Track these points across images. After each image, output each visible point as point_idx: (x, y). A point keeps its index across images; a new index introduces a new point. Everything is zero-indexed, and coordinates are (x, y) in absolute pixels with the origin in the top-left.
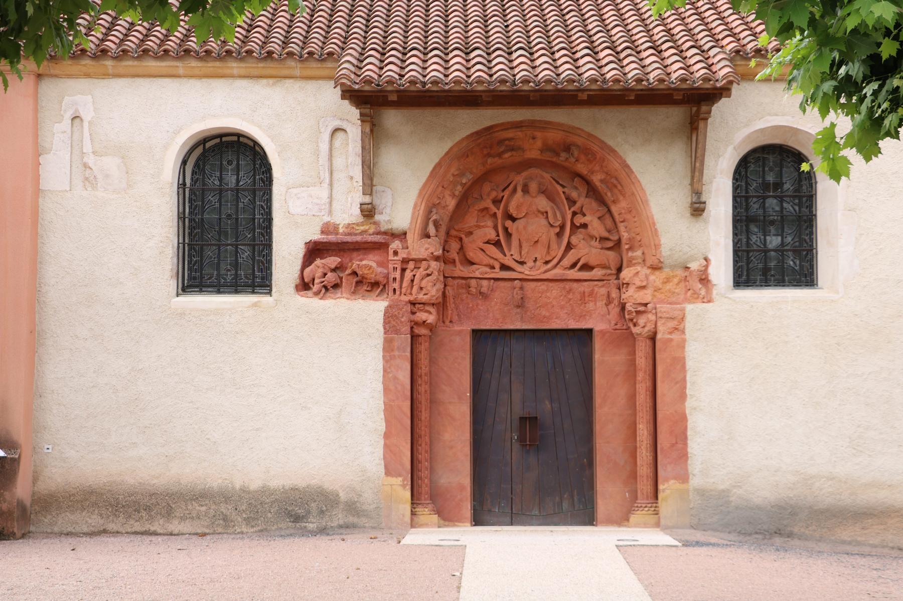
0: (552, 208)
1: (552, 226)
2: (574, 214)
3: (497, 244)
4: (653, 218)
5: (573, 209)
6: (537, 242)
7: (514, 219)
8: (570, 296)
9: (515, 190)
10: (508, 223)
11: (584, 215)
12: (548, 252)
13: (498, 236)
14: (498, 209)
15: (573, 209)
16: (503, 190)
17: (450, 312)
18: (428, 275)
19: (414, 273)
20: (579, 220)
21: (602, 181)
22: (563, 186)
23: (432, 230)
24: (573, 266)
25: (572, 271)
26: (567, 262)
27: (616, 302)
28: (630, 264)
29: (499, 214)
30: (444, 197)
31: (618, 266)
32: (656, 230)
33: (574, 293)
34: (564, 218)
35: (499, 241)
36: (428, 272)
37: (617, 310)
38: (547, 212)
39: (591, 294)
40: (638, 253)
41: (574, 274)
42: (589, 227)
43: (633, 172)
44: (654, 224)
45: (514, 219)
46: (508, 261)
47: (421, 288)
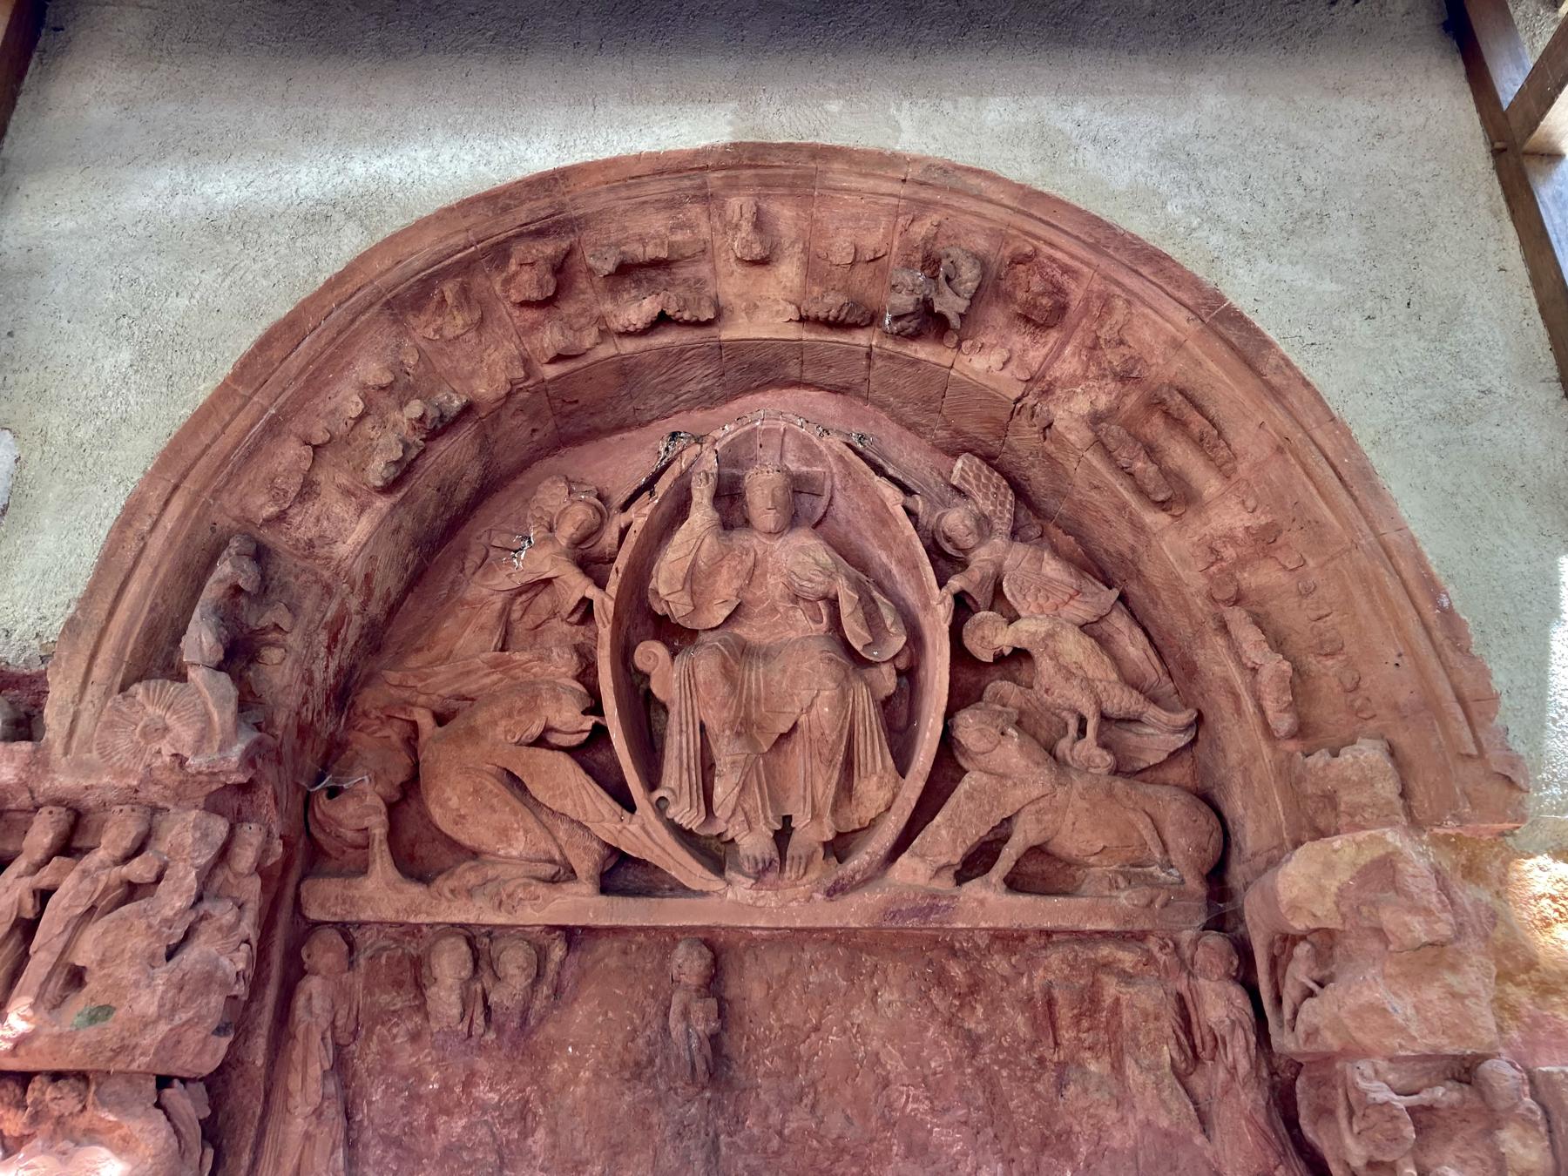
0: (858, 586)
1: (857, 660)
2: (963, 606)
3: (590, 751)
4: (1418, 557)
5: (956, 583)
6: (785, 737)
7: (676, 635)
8: (975, 1021)
9: (679, 509)
10: (651, 655)
11: (1013, 617)
12: (846, 787)
13: (596, 708)
14: (601, 584)
15: (956, 583)
16: (625, 507)
17: (299, 1124)
18: (132, 891)
19: (45, 878)
20: (991, 636)
21: (1096, 419)
22: (907, 491)
23: (201, 639)
24: (977, 861)
25: (974, 888)
26: (947, 836)
27: (1239, 1051)
28: (1314, 819)
29: (605, 602)
30: (308, 489)
31: (1212, 854)
32: (1448, 615)
33: (994, 1006)
34: (916, 639)
35: (599, 734)
36: (139, 870)
37: (1251, 1099)
38: (833, 603)
39: (1089, 1002)
40: (1368, 753)
41: (988, 904)
42: (1045, 665)
43: (1267, 344)
44: (1432, 587)
45: (676, 635)
46: (642, 835)
47: (77, 977)
